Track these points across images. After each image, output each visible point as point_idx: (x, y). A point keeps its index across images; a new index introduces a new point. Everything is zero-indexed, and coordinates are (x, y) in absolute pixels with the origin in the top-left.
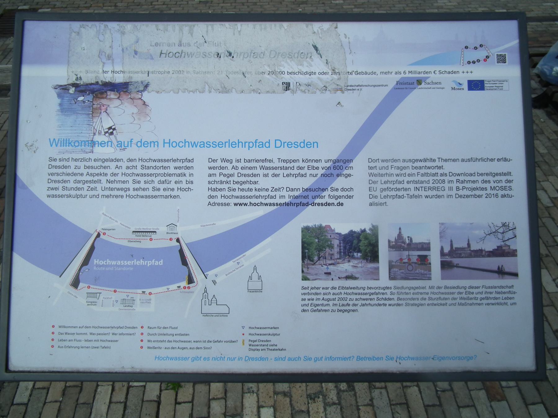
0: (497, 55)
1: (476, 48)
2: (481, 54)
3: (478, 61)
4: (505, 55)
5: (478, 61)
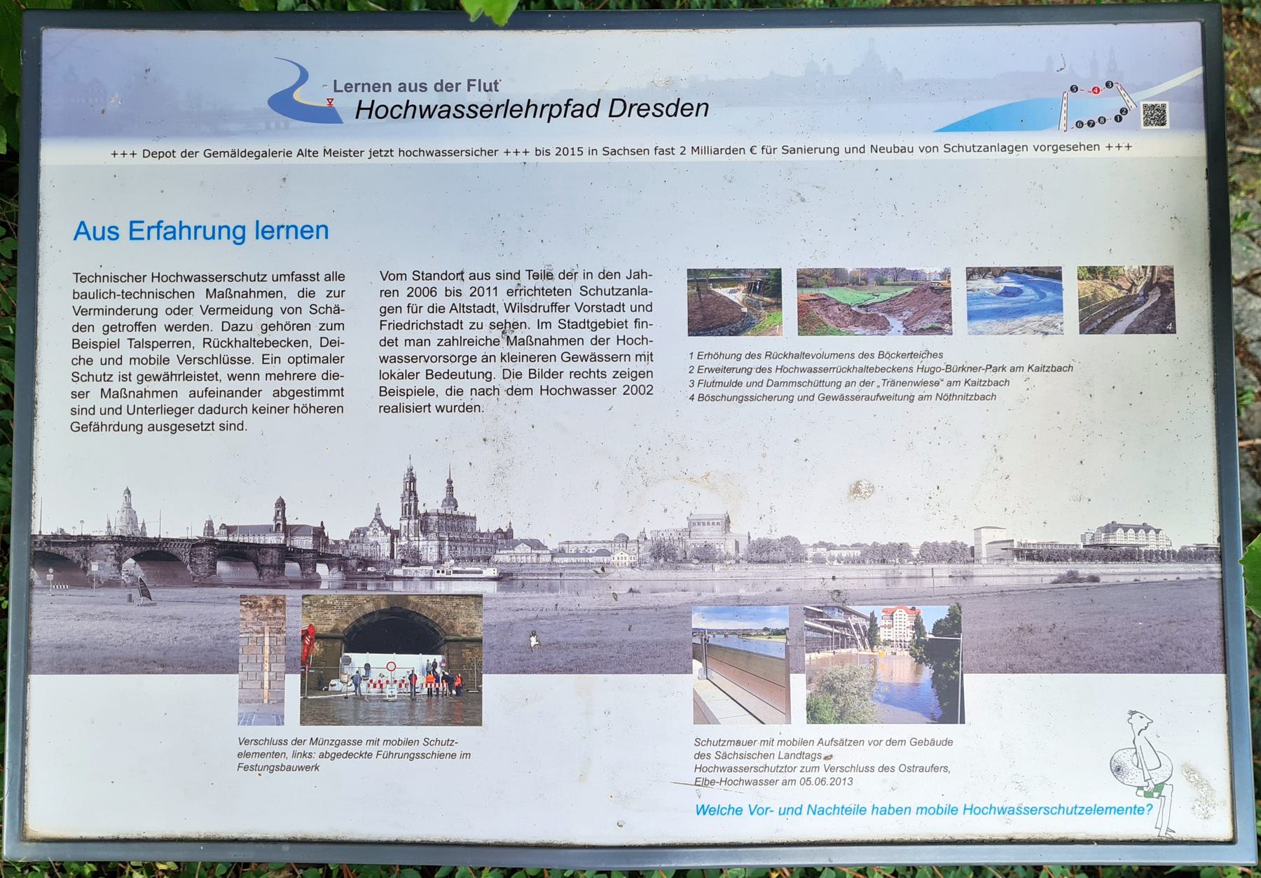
0: (1145, 106)
1: (1096, 90)
2: (1109, 104)
3: (1102, 120)
4: (1164, 106)
5: (1102, 120)
